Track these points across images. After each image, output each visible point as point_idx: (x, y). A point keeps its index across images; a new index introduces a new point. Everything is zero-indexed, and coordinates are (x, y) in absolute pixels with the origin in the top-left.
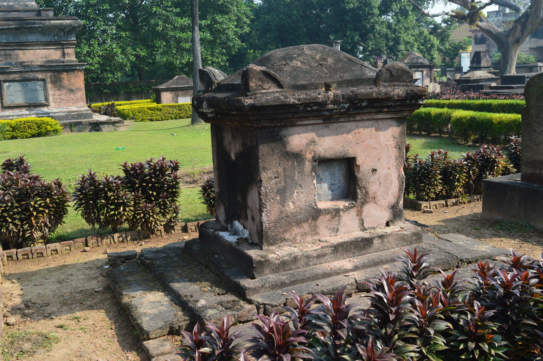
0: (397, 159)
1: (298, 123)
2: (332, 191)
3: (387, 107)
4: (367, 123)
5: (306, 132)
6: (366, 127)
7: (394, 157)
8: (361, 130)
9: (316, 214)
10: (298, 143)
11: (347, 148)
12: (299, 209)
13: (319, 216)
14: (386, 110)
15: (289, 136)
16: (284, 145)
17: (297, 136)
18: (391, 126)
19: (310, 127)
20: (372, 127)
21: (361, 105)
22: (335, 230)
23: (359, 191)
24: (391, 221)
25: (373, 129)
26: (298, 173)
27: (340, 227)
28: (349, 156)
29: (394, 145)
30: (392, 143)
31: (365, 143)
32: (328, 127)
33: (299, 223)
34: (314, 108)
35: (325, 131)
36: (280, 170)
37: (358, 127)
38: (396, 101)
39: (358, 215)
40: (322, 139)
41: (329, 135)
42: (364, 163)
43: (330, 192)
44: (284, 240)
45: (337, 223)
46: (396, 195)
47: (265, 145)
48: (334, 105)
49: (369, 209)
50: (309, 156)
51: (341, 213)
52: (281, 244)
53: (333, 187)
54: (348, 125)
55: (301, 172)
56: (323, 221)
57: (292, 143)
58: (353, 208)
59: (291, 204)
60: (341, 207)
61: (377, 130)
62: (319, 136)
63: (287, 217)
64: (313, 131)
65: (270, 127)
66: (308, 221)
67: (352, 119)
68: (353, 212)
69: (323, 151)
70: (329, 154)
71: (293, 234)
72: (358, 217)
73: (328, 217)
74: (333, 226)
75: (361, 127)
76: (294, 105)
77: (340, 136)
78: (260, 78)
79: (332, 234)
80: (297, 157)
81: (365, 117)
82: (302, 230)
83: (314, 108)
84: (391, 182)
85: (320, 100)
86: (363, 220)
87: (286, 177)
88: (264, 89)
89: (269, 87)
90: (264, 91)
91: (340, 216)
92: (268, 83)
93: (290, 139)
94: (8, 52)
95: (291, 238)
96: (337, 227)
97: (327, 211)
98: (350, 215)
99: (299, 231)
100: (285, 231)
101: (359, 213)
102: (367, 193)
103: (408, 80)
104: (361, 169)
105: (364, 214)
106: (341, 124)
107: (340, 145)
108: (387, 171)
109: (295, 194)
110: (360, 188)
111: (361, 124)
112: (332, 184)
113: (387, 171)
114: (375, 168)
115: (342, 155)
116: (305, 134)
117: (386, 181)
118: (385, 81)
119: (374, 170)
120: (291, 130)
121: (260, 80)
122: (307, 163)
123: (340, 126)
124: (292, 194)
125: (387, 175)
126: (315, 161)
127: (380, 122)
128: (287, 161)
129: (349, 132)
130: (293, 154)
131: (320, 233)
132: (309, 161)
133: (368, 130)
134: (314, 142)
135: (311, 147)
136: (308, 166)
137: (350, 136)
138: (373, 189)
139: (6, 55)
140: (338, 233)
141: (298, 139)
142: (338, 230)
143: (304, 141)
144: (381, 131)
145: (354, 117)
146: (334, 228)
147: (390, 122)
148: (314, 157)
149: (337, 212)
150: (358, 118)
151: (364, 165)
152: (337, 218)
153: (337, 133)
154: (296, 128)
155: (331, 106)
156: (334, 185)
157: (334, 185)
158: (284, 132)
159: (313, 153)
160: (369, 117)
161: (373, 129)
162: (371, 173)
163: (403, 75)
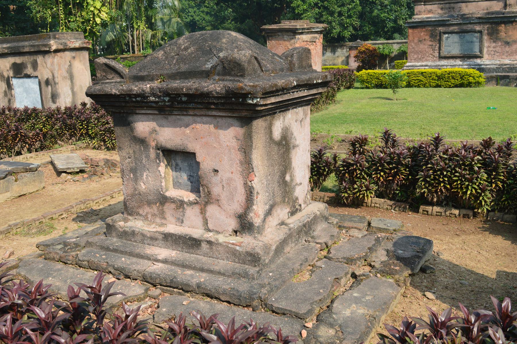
0: (241, 163)
1: (138, 111)
2: (191, 182)
3: (214, 104)
4: (205, 119)
5: (148, 121)
6: (204, 123)
7: (238, 162)
8: (199, 126)
9: (163, 200)
10: (142, 130)
11: (186, 142)
12: (148, 190)
13: (165, 202)
14: (213, 107)
15: (135, 122)
16: (132, 130)
17: (141, 123)
18: (232, 125)
19: (151, 117)
20: (211, 124)
21: (181, 99)
22: (180, 221)
23: (201, 189)
24: (239, 231)
25: (212, 126)
26: (145, 157)
27: (184, 219)
28: (188, 151)
29: (237, 147)
30: (234, 144)
31: (203, 140)
32: (167, 119)
33: (149, 203)
34: (138, 99)
35: (164, 122)
36: (131, 152)
37: (195, 122)
38: (218, 98)
39: (201, 213)
40: (163, 129)
41: (168, 127)
42: (206, 161)
43: (189, 183)
44: (138, 214)
45: (181, 214)
46: (242, 204)
47: (118, 128)
48: (155, 98)
49: (212, 210)
50: (153, 144)
51: (185, 205)
52: (136, 217)
53: (191, 178)
54: (187, 119)
55: (148, 157)
56: (169, 208)
57: (137, 129)
58: (197, 205)
59: (142, 184)
60: (186, 200)
61: (217, 127)
62: (160, 126)
63: (140, 195)
64: (153, 120)
65: (120, 113)
66: (156, 204)
67: (185, 113)
68: (197, 209)
69: (164, 141)
70: (169, 145)
71: (145, 211)
72: (202, 215)
73: (173, 206)
74: (178, 216)
75: (199, 123)
76: (115, 96)
77: (178, 129)
78: (103, 70)
79: (177, 223)
80: (142, 142)
81: (197, 112)
82: (152, 210)
83: (138, 99)
84: (236, 188)
85: (135, 93)
86: (207, 220)
87: (136, 158)
88: (109, 79)
89: (113, 77)
90: (108, 81)
91: (184, 208)
92: (111, 74)
93: (136, 125)
94: (452, 5)
95: (144, 214)
96: (182, 218)
97: (172, 200)
98: (194, 210)
99: (150, 210)
100: (139, 207)
101: (203, 212)
102: (209, 193)
103: (239, 74)
104: (201, 165)
105: (208, 214)
106: (178, 117)
107: (179, 138)
108: (230, 175)
109: (145, 176)
110: (202, 185)
111: (198, 119)
112: (191, 175)
113: (230, 175)
114: (216, 169)
115: (182, 148)
116: (147, 123)
117: (230, 186)
118: (218, 74)
119: (216, 171)
120: (136, 117)
121: (104, 71)
122: (151, 150)
123: (178, 119)
124: (142, 175)
125: (230, 180)
126: (159, 149)
127: (219, 120)
128: (135, 144)
129: (187, 126)
130: (139, 139)
131: (167, 218)
132: (153, 148)
133: (207, 126)
134: (156, 131)
135: (154, 135)
136: (152, 153)
137: (188, 131)
138: (216, 190)
139: (449, 8)
140: (183, 225)
141: (143, 126)
142: (182, 222)
143: (147, 129)
144: (221, 129)
145: (186, 111)
146: (179, 219)
147: (230, 120)
148: (157, 145)
149: (180, 204)
150: (191, 113)
151: (204, 163)
152: (181, 210)
153: (175, 125)
154: (140, 116)
155: (152, 99)
156: (193, 177)
157: (193, 177)
158: (131, 119)
159: (155, 141)
160: (202, 113)
161: (212, 126)
162: (213, 174)
163: (235, 67)
